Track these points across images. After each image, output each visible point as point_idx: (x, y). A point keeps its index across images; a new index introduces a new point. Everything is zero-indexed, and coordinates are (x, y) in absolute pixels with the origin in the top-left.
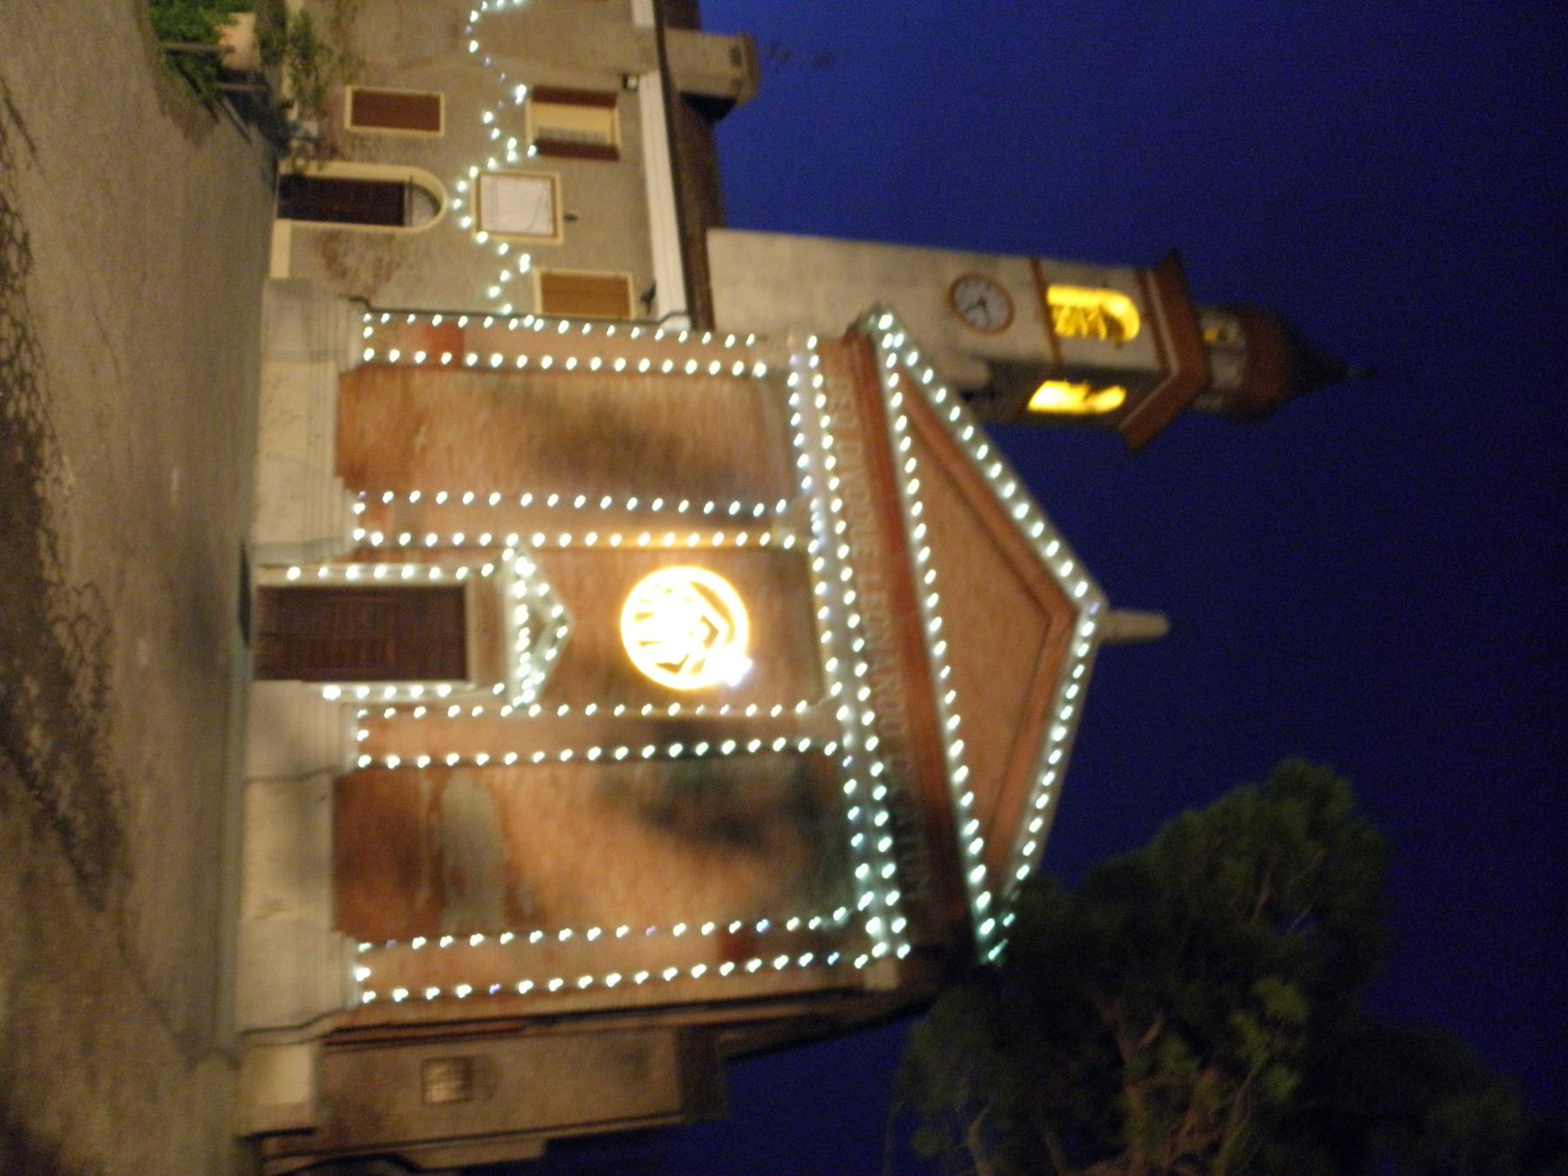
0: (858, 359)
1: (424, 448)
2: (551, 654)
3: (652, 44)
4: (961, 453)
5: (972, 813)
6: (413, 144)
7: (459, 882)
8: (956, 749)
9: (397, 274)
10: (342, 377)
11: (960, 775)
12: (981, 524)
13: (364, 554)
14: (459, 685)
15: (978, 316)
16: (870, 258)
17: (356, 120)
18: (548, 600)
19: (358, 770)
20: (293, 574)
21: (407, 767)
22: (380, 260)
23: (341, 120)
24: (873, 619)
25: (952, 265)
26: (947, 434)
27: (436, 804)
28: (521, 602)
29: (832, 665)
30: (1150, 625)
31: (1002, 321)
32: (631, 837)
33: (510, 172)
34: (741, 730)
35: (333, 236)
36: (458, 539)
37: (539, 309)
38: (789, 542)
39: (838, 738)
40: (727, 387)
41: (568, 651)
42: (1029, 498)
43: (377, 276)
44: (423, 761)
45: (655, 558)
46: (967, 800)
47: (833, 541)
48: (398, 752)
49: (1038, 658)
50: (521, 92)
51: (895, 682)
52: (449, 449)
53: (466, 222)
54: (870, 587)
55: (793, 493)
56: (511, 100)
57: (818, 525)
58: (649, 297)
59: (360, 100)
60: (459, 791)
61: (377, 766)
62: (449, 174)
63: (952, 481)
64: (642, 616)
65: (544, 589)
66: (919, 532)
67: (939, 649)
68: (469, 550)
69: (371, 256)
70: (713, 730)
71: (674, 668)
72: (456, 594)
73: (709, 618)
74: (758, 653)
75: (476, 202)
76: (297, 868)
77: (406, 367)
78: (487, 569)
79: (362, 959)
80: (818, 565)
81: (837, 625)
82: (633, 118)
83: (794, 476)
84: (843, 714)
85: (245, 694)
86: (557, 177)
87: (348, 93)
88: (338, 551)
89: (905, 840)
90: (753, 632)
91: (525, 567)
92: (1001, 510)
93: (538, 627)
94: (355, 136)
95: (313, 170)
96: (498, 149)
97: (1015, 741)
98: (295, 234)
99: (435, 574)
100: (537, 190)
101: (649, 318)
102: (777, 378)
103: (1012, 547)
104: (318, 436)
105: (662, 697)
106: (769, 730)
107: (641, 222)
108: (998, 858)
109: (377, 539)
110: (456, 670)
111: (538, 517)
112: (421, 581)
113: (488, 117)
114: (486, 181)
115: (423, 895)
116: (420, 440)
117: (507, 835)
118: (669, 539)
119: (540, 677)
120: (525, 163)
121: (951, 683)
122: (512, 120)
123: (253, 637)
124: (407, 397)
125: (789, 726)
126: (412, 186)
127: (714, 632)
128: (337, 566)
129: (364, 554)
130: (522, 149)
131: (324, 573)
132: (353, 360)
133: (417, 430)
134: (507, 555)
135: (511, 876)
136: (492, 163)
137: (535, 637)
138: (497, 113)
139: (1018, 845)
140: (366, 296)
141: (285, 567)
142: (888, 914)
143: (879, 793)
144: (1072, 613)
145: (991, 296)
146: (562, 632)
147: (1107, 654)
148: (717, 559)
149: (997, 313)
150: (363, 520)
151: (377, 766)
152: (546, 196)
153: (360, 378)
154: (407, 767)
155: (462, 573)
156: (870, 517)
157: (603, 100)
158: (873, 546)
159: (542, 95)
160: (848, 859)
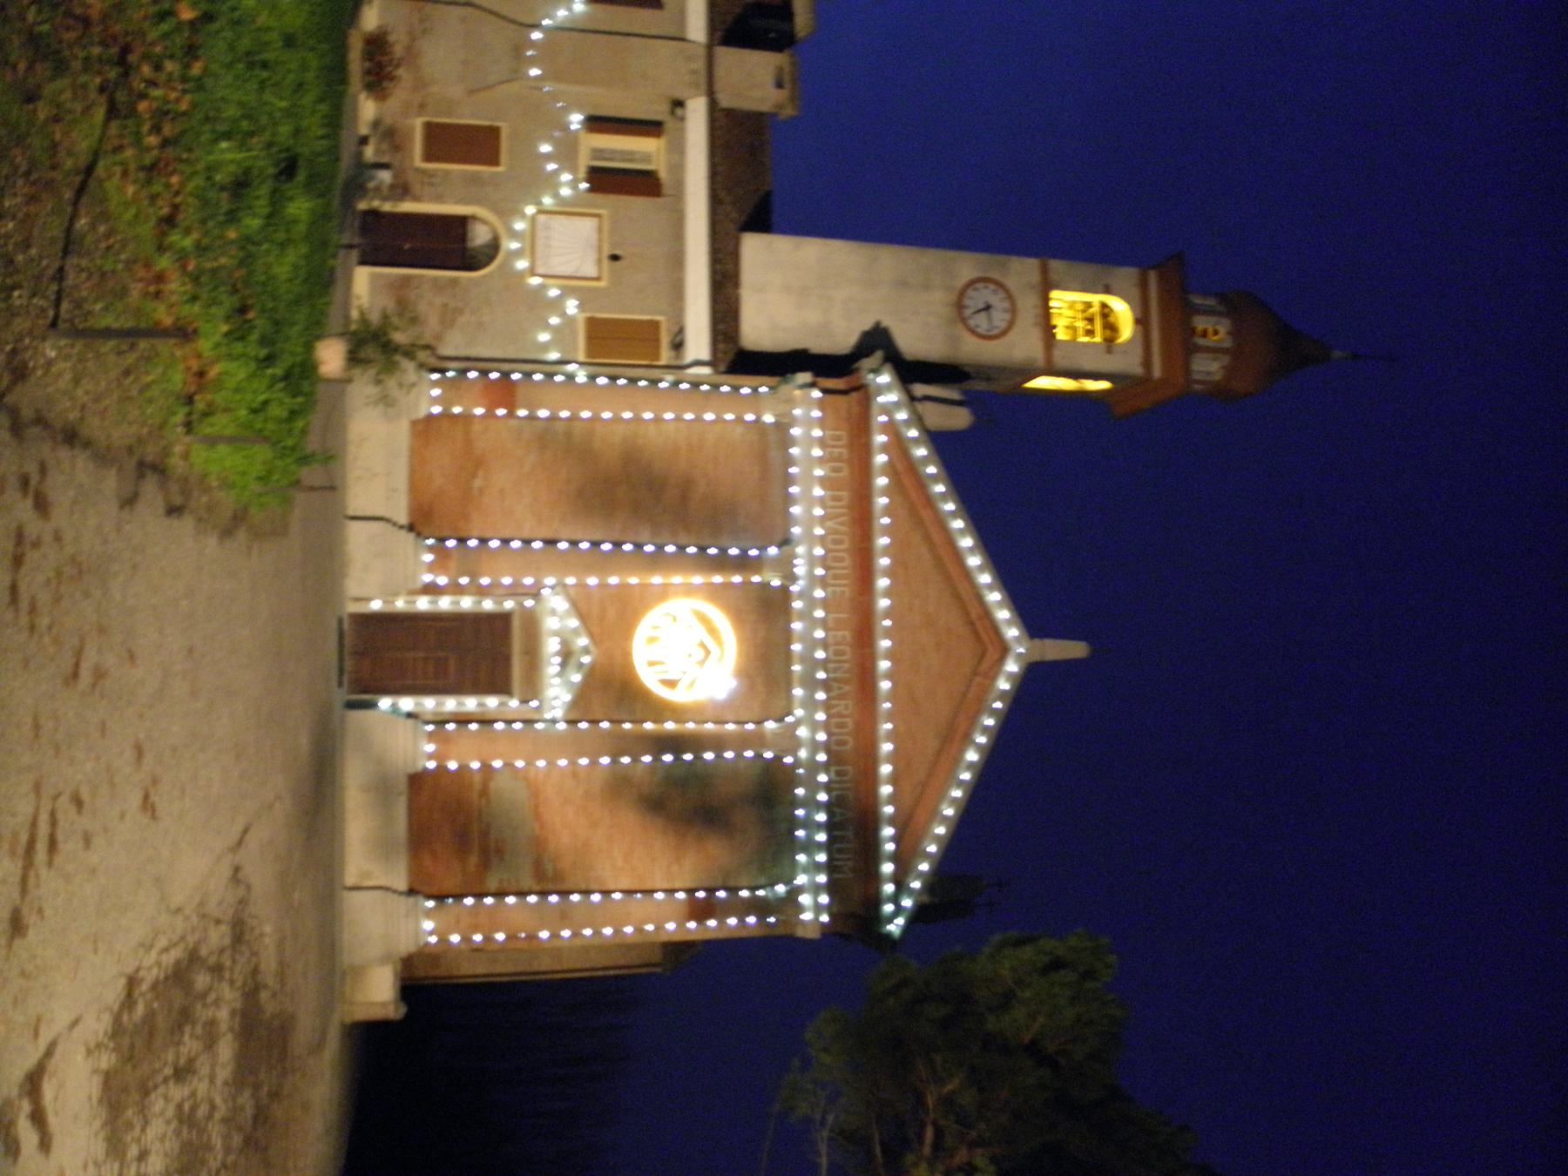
0: (856, 409)
1: (481, 491)
2: (577, 678)
3: (700, 65)
4: (930, 501)
5: (892, 821)
6: (475, 180)
7: (500, 851)
8: (886, 769)
9: (463, 319)
10: (414, 423)
11: (886, 790)
12: (938, 562)
13: (431, 590)
14: (504, 698)
15: (981, 322)
16: (890, 260)
17: (429, 156)
18: (575, 632)
19: (426, 770)
20: (376, 605)
21: (463, 768)
22: (445, 305)
23: (412, 158)
24: (837, 653)
25: (966, 266)
26: (922, 483)
27: (484, 792)
28: (556, 633)
29: (798, 692)
30: (1075, 649)
31: (1003, 325)
32: (630, 818)
33: (566, 210)
34: (718, 743)
35: (407, 280)
36: (507, 581)
37: (582, 357)
38: (776, 582)
39: (794, 752)
40: (739, 430)
41: (591, 674)
42: (982, 554)
43: (442, 322)
44: (475, 765)
45: (664, 593)
46: (889, 810)
47: (813, 581)
48: (458, 760)
49: (968, 687)
50: (576, 120)
51: (847, 707)
52: (502, 491)
53: (522, 264)
54: (839, 625)
55: (785, 541)
56: (565, 127)
57: (800, 569)
58: (678, 346)
59: (432, 130)
60: (500, 784)
61: (442, 768)
62: (508, 211)
63: (919, 523)
64: (652, 640)
65: (574, 623)
66: (883, 583)
67: (885, 685)
68: (516, 591)
69: (438, 301)
70: (696, 743)
71: (671, 684)
72: (503, 619)
73: (706, 643)
74: (743, 673)
75: (531, 241)
76: (382, 847)
77: (467, 418)
78: (529, 603)
79: (429, 914)
80: (797, 605)
81: (807, 659)
82: (678, 149)
83: (788, 520)
84: (803, 732)
85: (343, 720)
86: (602, 284)
87: (418, 123)
88: (411, 587)
89: (837, 833)
90: (740, 654)
91: (559, 603)
92: (958, 556)
93: (567, 655)
94: (424, 172)
95: (387, 207)
96: (551, 182)
97: (939, 753)
98: (373, 276)
99: (488, 605)
100: (585, 228)
101: (678, 363)
102: (782, 427)
103: (963, 589)
104: (394, 490)
105: (661, 710)
106: (742, 742)
107: (677, 261)
108: (904, 863)
109: (442, 580)
110: (501, 686)
111: (576, 561)
112: (477, 609)
113: (545, 148)
114: (541, 270)
115: (473, 860)
116: (478, 483)
117: (537, 816)
118: (677, 579)
119: (567, 697)
120: (575, 201)
121: (890, 716)
122: (567, 153)
123: (346, 679)
124: (468, 443)
125: (758, 740)
126: (474, 218)
127: (708, 652)
128: (411, 598)
129: (431, 590)
130: (573, 184)
131: (400, 604)
132: (422, 413)
133: (474, 476)
134: (545, 592)
135: (538, 845)
136: (547, 201)
137: (563, 665)
138: (556, 143)
139: (926, 843)
140: (433, 343)
141: (368, 600)
142: (816, 889)
143: (822, 797)
144: (1004, 649)
145: (997, 300)
146: (586, 659)
147: (1033, 673)
148: (713, 593)
149: (999, 318)
150: (431, 568)
151: (442, 768)
152: (594, 236)
153: (426, 428)
154: (463, 768)
155: (509, 605)
156: (847, 562)
157: (650, 127)
158: (846, 589)
159: (597, 123)
160: (794, 846)
